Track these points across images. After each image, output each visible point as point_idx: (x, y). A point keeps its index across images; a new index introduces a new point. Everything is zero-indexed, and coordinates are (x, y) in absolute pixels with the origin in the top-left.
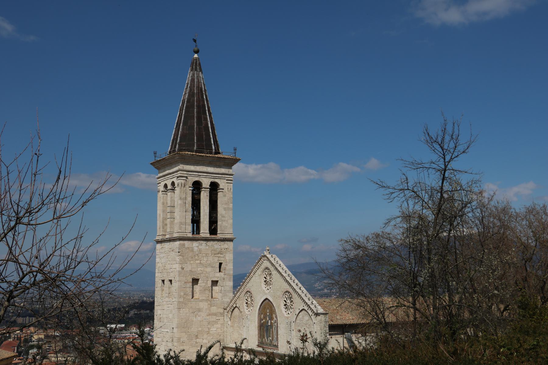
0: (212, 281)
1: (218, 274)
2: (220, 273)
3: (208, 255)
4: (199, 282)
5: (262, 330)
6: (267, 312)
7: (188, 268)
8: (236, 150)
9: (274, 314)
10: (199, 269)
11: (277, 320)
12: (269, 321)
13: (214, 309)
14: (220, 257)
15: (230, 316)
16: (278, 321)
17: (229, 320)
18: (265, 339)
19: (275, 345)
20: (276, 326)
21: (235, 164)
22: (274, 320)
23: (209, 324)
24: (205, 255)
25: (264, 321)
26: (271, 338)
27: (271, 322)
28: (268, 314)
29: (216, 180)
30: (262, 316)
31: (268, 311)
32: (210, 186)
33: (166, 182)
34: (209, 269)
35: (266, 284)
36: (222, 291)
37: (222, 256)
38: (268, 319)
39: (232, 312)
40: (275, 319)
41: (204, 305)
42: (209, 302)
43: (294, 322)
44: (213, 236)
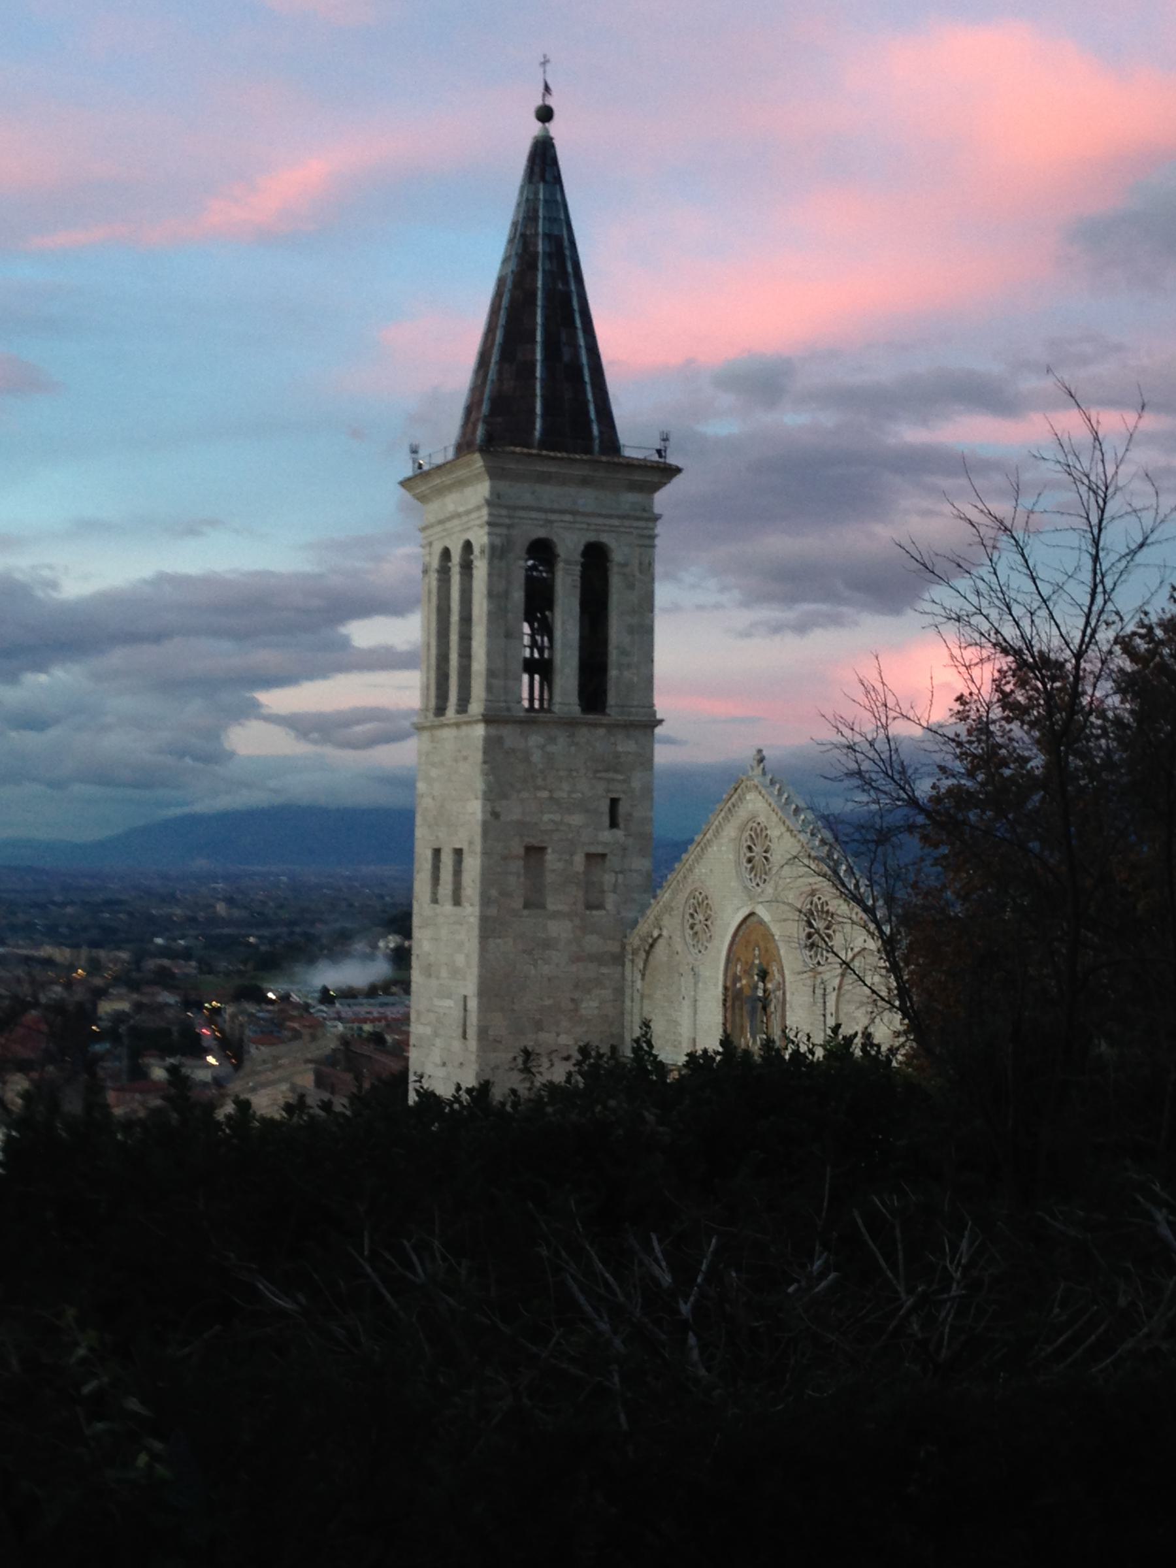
0: (589, 856)
1: (606, 835)
2: (615, 830)
3: (575, 774)
5: (737, 1011)
6: (755, 955)
7: (513, 812)
10: (546, 817)
11: (784, 982)
13: (593, 942)
14: (613, 780)
15: (641, 966)
16: (787, 984)
17: (640, 976)
18: (745, 1037)
21: (665, 484)
22: (775, 982)
23: (576, 986)
27: (765, 985)
29: (605, 538)
30: (739, 967)
31: (757, 952)
34: (576, 819)
35: (752, 869)
37: (620, 777)
39: (648, 953)
40: (777, 976)
41: (559, 929)
43: (834, 989)
44: (591, 717)
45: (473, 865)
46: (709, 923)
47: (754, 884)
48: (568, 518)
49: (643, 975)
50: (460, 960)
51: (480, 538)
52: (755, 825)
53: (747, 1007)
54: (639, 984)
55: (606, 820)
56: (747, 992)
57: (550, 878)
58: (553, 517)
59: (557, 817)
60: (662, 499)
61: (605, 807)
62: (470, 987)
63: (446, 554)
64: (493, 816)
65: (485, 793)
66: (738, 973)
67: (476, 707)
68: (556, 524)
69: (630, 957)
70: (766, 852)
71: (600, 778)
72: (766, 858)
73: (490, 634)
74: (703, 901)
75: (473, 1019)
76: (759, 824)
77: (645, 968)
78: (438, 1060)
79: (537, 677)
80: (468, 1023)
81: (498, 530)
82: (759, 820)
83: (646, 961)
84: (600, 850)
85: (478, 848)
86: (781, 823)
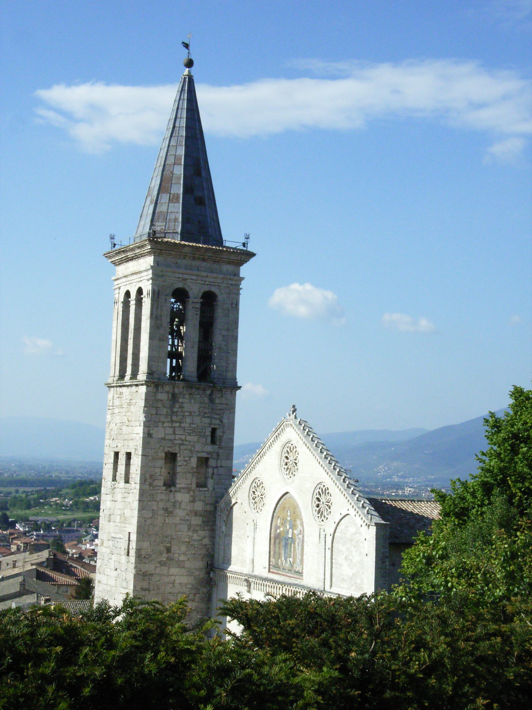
0: (199, 458)
1: (209, 448)
3: (193, 414)
4: (179, 459)
5: (277, 545)
6: (288, 515)
8: (248, 238)
9: (298, 520)
11: (303, 530)
12: (291, 531)
15: (225, 519)
16: (305, 531)
17: (224, 524)
18: (281, 560)
20: (301, 539)
21: (246, 262)
24: (188, 414)
25: (281, 529)
26: (291, 560)
27: (293, 531)
28: (289, 519)
29: (213, 289)
30: (279, 521)
32: (202, 297)
36: (214, 477)
38: (288, 527)
40: (300, 527)
41: (182, 497)
42: (192, 493)
43: (331, 535)
45: (136, 462)
46: (263, 497)
47: (289, 477)
48: (194, 277)
50: (128, 513)
51: (147, 287)
52: (290, 445)
53: (283, 543)
54: (224, 528)
55: (209, 439)
57: (179, 469)
59: (183, 437)
60: (245, 270)
61: (208, 433)
62: (133, 528)
63: (128, 294)
64: (148, 436)
65: (144, 422)
66: (278, 525)
67: (142, 376)
69: (219, 514)
70: (295, 460)
71: (206, 417)
72: (296, 464)
73: (151, 338)
74: (260, 485)
75: (133, 545)
76: (292, 445)
78: (113, 568)
79: (174, 361)
80: (130, 547)
82: (292, 443)
84: (205, 455)
85: (140, 453)
86: (304, 445)
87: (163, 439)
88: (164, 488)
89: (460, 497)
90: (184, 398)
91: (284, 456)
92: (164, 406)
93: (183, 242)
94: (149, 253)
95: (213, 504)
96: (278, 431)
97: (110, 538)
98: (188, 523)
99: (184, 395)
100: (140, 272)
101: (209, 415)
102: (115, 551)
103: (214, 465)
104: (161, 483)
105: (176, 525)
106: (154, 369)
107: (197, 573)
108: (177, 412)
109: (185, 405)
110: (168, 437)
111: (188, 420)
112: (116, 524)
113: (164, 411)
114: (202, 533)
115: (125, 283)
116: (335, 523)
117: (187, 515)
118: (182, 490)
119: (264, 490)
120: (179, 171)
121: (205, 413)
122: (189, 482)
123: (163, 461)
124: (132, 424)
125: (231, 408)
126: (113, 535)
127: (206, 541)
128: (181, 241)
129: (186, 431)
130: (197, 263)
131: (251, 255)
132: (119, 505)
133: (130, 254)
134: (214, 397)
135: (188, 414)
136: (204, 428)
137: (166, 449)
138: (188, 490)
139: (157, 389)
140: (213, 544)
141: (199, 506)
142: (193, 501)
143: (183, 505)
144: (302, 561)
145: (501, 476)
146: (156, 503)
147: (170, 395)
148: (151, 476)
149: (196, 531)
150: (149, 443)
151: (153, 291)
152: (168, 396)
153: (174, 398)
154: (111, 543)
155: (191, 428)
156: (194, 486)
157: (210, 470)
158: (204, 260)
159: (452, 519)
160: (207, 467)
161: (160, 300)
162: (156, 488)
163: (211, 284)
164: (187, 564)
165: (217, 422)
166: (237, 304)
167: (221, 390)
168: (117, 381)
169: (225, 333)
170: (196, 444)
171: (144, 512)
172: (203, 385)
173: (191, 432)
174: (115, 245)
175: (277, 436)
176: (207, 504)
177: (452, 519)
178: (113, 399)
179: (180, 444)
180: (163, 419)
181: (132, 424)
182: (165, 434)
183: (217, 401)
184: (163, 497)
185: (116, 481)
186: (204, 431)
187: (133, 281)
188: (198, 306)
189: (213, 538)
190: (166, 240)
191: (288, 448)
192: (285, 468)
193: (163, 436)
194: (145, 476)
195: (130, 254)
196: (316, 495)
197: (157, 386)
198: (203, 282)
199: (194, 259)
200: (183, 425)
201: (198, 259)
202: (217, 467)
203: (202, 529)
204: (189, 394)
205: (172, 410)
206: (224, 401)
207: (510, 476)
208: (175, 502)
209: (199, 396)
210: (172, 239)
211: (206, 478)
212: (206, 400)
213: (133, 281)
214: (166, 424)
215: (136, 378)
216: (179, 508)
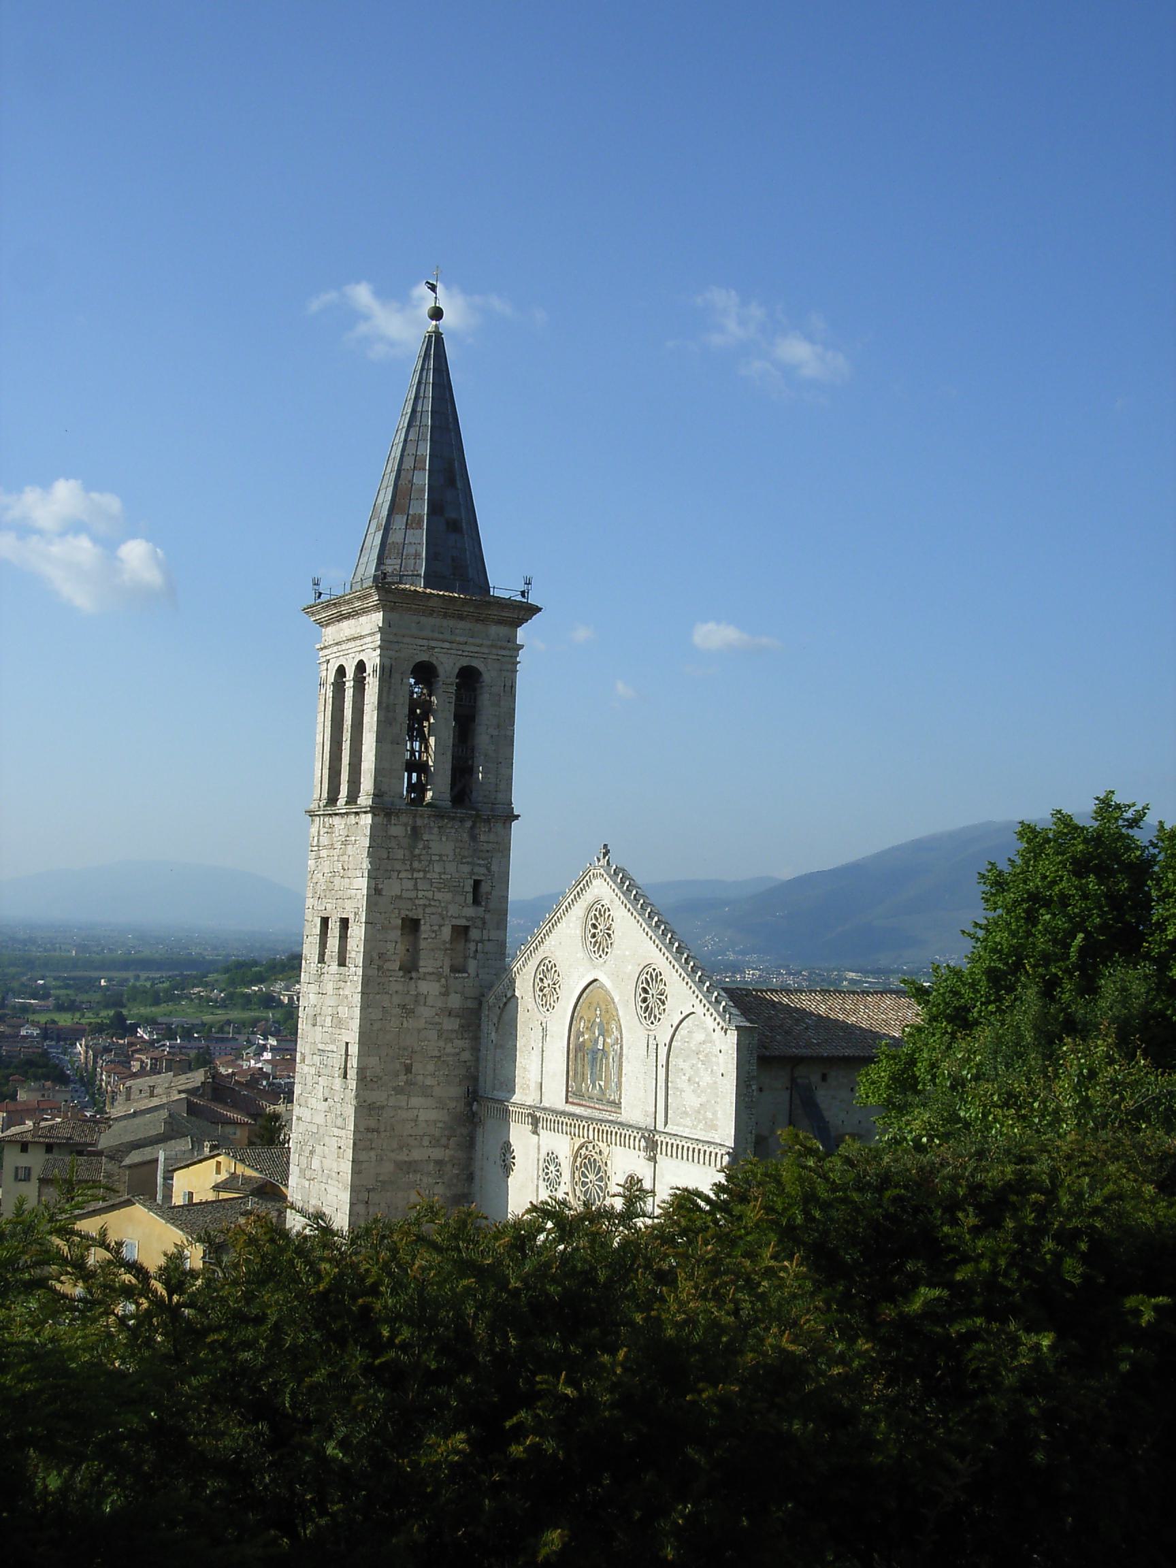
1: (470, 911)
3: (445, 858)
4: (423, 928)
8: (529, 584)
11: (621, 1038)
12: (601, 1038)
15: (495, 1020)
16: (624, 1040)
18: (586, 1084)
19: (613, 1102)
20: (619, 1051)
22: (613, 1036)
24: (437, 858)
27: (604, 1041)
28: (598, 1020)
29: (475, 663)
30: (582, 1024)
31: (598, 1012)
32: (459, 675)
33: (342, 661)
36: (478, 956)
38: (597, 1034)
39: (502, 1009)
40: (616, 1033)
41: (429, 988)
43: (665, 1045)
45: (357, 933)
46: (557, 986)
47: (597, 956)
48: (447, 645)
49: (497, 1029)
50: (344, 1012)
51: (373, 659)
52: (599, 906)
53: (588, 1058)
55: (470, 898)
56: (589, 1045)
58: (433, 644)
59: (430, 894)
60: (522, 634)
62: (351, 1035)
63: (341, 671)
64: (375, 892)
66: (581, 1029)
67: (365, 800)
68: (436, 650)
69: (487, 1013)
70: (609, 929)
71: (464, 863)
72: (609, 935)
73: (379, 740)
74: (552, 968)
75: (353, 1062)
76: (603, 906)
77: (499, 1022)
78: (320, 1096)
79: (414, 775)
81: (391, 653)
82: (603, 903)
83: (500, 1018)
84: (463, 922)
87: (400, 897)
88: (401, 973)
89: (951, 991)
90: (431, 833)
91: (590, 923)
92: (400, 847)
93: (428, 591)
94: (376, 608)
95: (476, 998)
96: (582, 884)
97: (316, 1052)
98: (438, 1027)
99: (430, 828)
100: (361, 637)
101: (469, 860)
102: (323, 1071)
103: (478, 939)
104: (396, 966)
105: (419, 1031)
106: (384, 788)
107: (452, 1105)
108: (420, 855)
109: (432, 844)
110: (405, 895)
111: (438, 868)
112: (325, 1029)
113: (400, 854)
114: (459, 1043)
115: (338, 654)
116: (672, 1026)
117: (436, 1014)
118: (428, 977)
119: (559, 976)
120: (423, 479)
121: (464, 857)
122: (439, 963)
123: (399, 932)
124: (350, 874)
125: (504, 849)
126: (321, 1046)
127: (466, 1056)
128: (425, 588)
129: (434, 885)
130: (451, 623)
131: (536, 610)
132: (330, 1001)
133: (345, 609)
134: (477, 831)
135: (437, 858)
136: (461, 880)
137: (404, 913)
138: (438, 976)
139: (389, 820)
140: (477, 1060)
141: (455, 1001)
142: (445, 994)
143: (430, 1001)
144: (619, 1084)
145: (1014, 958)
146: (387, 996)
147: (409, 829)
148: (381, 956)
149: (451, 1040)
150: (376, 904)
151: (383, 667)
152: (406, 830)
153: (415, 833)
154: (317, 1059)
155: (442, 881)
156: (447, 970)
157: (472, 946)
158: (461, 618)
159: (943, 1025)
160: (467, 940)
161: (393, 681)
162: (388, 974)
163: (472, 655)
164: (437, 1091)
165: (483, 870)
166: (513, 687)
167: (488, 821)
168: (324, 807)
169: (495, 733)
170: (450, 906)
171: (370, 1010)
172: (460, 812)
173: (443, 886)
174: (320, 594)
175: (578, 893)
176: (467, 998)
177: (943, 1025)
178: (319, 835)
179: (425, 905)
180: (398, 866)
181: (350, 874)
182: (402, 890)
183: (482, 838)
184: (399, 987)
185: (325, 963)
186: (462, 884)
187: (350, 651)
188: (453, 689)
189: (476, 1050)
190: (403, 586)
191: (596, 910)
192: (591, 942)
193: (399, 894)
194: (371, 956)
195: (345, 609)
196: (642, 983)
197: (388, 815)
198: (460, 653)
199: (445, 616)
200: (428, 876)
201: (453, 616)
202: (482, 941)
203: (460, 1037)
204: (439, 827)
205: (412, 852)
206: (492, 837)
207: (1027, 957)
208: (417, 996)
209: (454, 831)
210: (411, 585)
211: (466, 958)
212: (465, 836)
213: (350, 651)
214: (403, 875)
215: (355, 803)
216: (425, 1005)
